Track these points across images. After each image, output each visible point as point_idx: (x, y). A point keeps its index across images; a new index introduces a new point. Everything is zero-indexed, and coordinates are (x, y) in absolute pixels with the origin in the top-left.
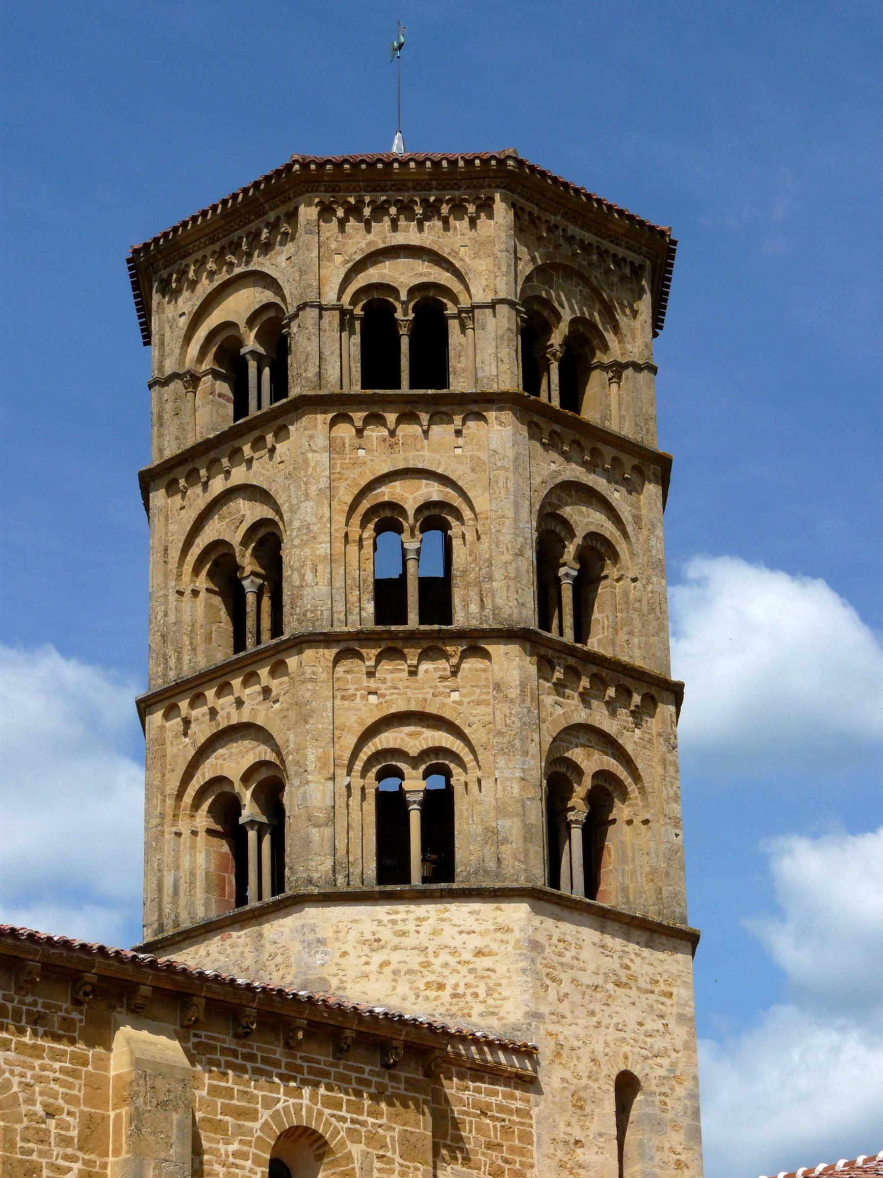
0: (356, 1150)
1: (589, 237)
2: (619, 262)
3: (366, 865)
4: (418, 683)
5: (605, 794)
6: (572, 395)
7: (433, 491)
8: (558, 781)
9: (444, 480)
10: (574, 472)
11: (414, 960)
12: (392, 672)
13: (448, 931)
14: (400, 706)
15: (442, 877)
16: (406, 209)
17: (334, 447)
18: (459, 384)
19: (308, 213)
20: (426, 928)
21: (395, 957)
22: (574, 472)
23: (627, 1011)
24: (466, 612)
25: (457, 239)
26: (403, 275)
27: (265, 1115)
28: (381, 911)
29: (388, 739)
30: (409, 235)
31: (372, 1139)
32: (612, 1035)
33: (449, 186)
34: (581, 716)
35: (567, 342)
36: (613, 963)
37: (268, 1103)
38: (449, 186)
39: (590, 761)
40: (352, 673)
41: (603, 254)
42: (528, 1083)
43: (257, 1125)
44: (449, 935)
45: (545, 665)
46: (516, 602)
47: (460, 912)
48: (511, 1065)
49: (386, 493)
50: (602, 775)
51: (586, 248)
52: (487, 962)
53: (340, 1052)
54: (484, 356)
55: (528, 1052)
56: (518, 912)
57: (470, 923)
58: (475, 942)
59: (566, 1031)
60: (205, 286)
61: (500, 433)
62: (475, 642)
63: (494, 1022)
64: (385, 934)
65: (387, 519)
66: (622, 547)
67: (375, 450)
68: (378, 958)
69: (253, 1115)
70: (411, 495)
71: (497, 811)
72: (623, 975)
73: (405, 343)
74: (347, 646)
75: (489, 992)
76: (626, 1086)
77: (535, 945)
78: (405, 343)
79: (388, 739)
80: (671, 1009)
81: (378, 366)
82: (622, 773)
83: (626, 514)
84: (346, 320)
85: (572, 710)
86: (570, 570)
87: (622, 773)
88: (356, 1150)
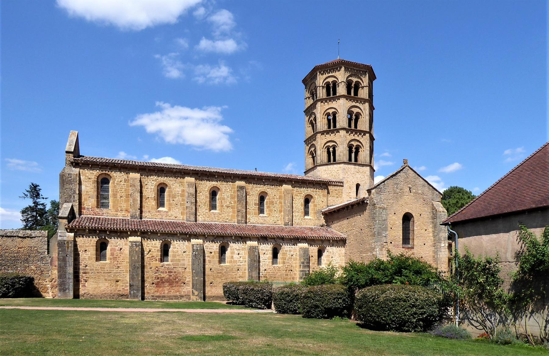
0: (316, 196)
1: (358, 69)
2: (363, 71)
3: (325, 160)
6: (356, 93)
7: (334, 110)
8: (350, 147)
9: (335, 109)
10: (354, 104)
11: (330, 172)
15: (335, 162)
17: (321, 106)
18: (337, 95)
19: (318, 73)
22: (354, 104)
23: (358, 176)
24: (338, 126)
29: (328, 144)
30: (330, 74)
34: (353, 138)
35: (355, 85)
39: (355, 144)
40: (323, 136)
41: (360, 71)
44: (334, 169)
45: (347, 132)
47: (335, 166)
49: (328, 111)
51: (357, 70)
53: (314, 185)
54: (342, 90)
55: (342, 182)
56: (342, 165)
59: (349, 180)
60: (310, 84)
61: (342, 101)
62: (338, 131)
65: (328, 115)
66: (362, 113)
67: (327, 106)
70: (331, 111)
71: (342, 152)
74: (323, 133)
76: (358, 186)
77: (344, 169)
79: (328, 144)
80: (365, 174)
81: (328, 94)
82: (360, 145)
83: (362, 109)
84: (323, 87)
85: (352, 137)
86: (354, 118)
87: (360, 145)
88: (316, 196)
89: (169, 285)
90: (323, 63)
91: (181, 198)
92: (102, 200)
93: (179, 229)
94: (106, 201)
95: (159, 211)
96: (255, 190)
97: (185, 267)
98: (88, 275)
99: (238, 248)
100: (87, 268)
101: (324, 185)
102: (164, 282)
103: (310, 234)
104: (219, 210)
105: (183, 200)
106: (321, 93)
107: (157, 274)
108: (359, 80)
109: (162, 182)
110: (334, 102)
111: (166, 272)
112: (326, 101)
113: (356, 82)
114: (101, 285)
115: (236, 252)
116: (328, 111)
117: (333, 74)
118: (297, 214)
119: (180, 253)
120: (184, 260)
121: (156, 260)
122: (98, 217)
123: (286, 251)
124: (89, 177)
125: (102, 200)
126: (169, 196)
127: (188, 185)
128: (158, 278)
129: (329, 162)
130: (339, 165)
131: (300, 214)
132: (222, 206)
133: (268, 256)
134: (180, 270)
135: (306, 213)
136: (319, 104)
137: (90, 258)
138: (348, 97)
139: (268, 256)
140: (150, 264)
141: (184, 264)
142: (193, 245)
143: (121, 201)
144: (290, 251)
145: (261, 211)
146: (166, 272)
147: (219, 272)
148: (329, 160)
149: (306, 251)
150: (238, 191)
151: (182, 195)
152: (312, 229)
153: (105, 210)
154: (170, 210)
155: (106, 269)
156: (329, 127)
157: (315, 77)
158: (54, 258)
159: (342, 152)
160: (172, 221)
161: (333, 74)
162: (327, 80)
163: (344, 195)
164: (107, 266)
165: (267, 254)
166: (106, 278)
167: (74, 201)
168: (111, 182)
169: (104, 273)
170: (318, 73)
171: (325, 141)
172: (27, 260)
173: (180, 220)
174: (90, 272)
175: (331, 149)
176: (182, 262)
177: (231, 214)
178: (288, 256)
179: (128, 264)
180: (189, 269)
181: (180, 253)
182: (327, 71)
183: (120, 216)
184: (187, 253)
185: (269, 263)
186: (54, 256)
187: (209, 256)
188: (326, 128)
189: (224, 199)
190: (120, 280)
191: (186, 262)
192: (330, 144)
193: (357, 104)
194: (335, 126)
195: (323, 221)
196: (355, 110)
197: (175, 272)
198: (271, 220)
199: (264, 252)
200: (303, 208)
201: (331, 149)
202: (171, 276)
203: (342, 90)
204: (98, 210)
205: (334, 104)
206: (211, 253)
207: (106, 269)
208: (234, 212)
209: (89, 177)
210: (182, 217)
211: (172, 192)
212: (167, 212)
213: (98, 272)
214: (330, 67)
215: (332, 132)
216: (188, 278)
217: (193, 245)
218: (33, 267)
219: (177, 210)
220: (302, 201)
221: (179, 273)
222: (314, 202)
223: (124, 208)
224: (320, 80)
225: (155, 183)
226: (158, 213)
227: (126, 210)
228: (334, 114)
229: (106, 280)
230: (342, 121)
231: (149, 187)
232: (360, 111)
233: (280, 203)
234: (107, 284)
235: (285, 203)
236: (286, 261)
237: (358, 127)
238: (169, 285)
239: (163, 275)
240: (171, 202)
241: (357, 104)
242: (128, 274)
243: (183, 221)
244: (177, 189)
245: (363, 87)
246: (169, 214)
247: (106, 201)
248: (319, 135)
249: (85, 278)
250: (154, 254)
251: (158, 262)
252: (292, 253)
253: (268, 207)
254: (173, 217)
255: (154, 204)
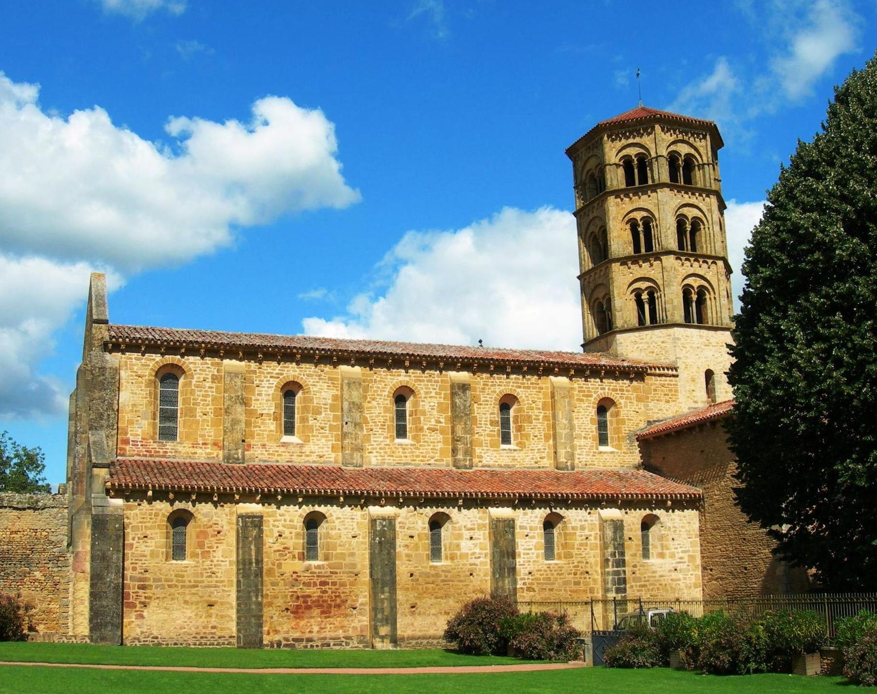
0: (622, 401)
3: (634, 322)
4: (644, 269)
5: (701, 291)
7: (645, 214)
11: (645, 346)
12: (635, 267)
13: (654, 337)
14: (639, 276)
15: (656, 323)
16: (631, 133)
17: (617, 205)
19: (606, 138)
20: (648, 337)
21: (641, 346)
24: (656, 248)
25: (647, 140)
26: (633, 152)
27: (595, 396)
28: (637, 334)
31: (627, 398)
32: (704, 360)
33: (645, 123)
36: (704, 340)
37: (595, 393)
38: (645, 123)
42: (677, 376)
43: (592, 399)
44: (655, 338)
46: (672, 243)
47: (657, 332)
48: (671, 371)
49: (632, 215)
50: (701, 287)
52: (665, 345)
54: (661, 172)
57: (660, 335)
58: (662, 339)
61: (664, 194)
62: (658, 257)
63: (667, 361)
64: (637, 340)
66: (704, 219)
67: (627, 204)
68: (636, 346)
69: (591, 396)
70: (638, 215)
72: (707, 343)
73: (636, 171)
74: (624, 261)
75: (666, 352)
78: (636, 171)
81: (630, 180)
83: (705, 209)
88: (622, 401)
89: (323, 612)
90: (615, 119)
91: (331, 415)
92: (167, 423)
93: (340, 486)
94: (171, 424)
95: (284, 445)
96: (489, 389)
97: (356, 571)
98: (149, 593)
99: (469, 526)
100: (147, 575)
101: (636, 373)
102: (309, 608)
103: (624, 490)
104: (415, 438)
105: (335, 418)
106: (616, 178)
107: (295, 589)
108: (693, 151)
109: (291, 379)
110: (645, 197)
111: (315, 584)
112: (627, 196)
113: (686, 155)
114: (176, 614)
115: (467, 534)
116: (632, 215)
117: (637, 140)
118: (582, 442)
119: (344, 539)
120: (352, 555)
121: (294, 557)
122: (157, 459)
123: (573, 528)
124: (135, 373)
125: (167, 423)
126: (305, 409)
127: (349, 384)
128: (298, 597)
129: (641, 326)
130: (664, 331)
131: (590, 441)
132: (421, 429)
133: (535, 541)
134: (345, 578)
135: (603, 440)
136: (612, 201)
137: (153, 554)
138: (673, 184)
139: (535, 541)
140: (280, 566)
141: (354, 565)
142: (373, 521)
143: (203, 425)
144: (583, 528)
145: (506, 439)
146: (315, 584)
147: (431, 579)
148: (641, 321)
149: (618, 526)
150: (453, 394)
151: (333, 408)
152: (621, 478)
153: (169, 445)
154: (307, 440)
155: (186, 579)
156: (637, 248)
157: (600, 145)
158: (80, 555)
159: (672, 302)
160: (314, 465)
161: (637, 140)
162: (624, 152)
163: (682, 397)
164: (190, 571)
165: (533, 537)
166: (187, 598)
167: (108, 426)
168: (182, 381)
169: (183, 587)
170: (606, 138)
171: (631, 278)
172: (26, 560)
173: (330, 462)
174: (154, 584)
175: (645, 296)
176: (348, 560)
177: (440, 446)
178: (578, 541)
179: (234, 567)
180: (365, 577)
181: (344, 539)
182: (624, 135)
183: (203, 455)
184: (360, 539)
185: (537, 557)
186: (80, 549)
187: (407, 546)
188: (630, 250)
189: (424, 413)
190: (216, 602)
191: (357, 560)
192: (643, 285)
193: (693, 200)
194: (649, 247)
195: (636, 457)
196: (691, 213)
197: (334, 584)
198: (527, 456)
199: (526, 532)
200: (594, 427)
201: (645, 296)
202: (325, 592)
203: (661, 172)
204: (155, 445)
205: (644, 201)
206: (412, 537)
207: (186, 579)
208: (445, 442)
209: (135, 373)
210: (333, 455)
211: (311, 400)
212: (301, 446)
213: (170, 586)
214: (629, 126)
215: (646, 259)
216: (363, 597)
217: (373, 521)
218: (38, 574)
219: (323, 440)
220: (593, 412)
221: (343, 585)
222: (617, 414)
223: (210, 440)
224: (613, 151)
225: (274, 382)
226: (283, 449)
227: (215, 444)
228: (647, 222)
229: (186, 602)
230: (667, 235)
231: (264, 391)
232: (700, 215)
233: (546, 418)
234: (189, 613)
235: (554, 417)
236: (575, 552)
237: (698, 247)
238: (323, 612)
239: (308, 591)
240: (311, 423)
241: (693, 200)
242: (234, 589)
243: (336, 466)
244: (324, 394)
245: (702, 166)
246: (306, 449)
247: (171, 424)
248: (616, 267)
249: (143, 599)
250: (290, 544)
251: (297, 560)
252: (587, 532)
253: (519, 429)
254: (314, 458)
255: (273, 427)
